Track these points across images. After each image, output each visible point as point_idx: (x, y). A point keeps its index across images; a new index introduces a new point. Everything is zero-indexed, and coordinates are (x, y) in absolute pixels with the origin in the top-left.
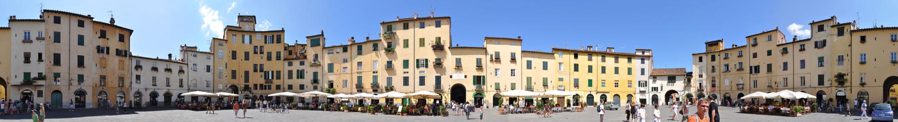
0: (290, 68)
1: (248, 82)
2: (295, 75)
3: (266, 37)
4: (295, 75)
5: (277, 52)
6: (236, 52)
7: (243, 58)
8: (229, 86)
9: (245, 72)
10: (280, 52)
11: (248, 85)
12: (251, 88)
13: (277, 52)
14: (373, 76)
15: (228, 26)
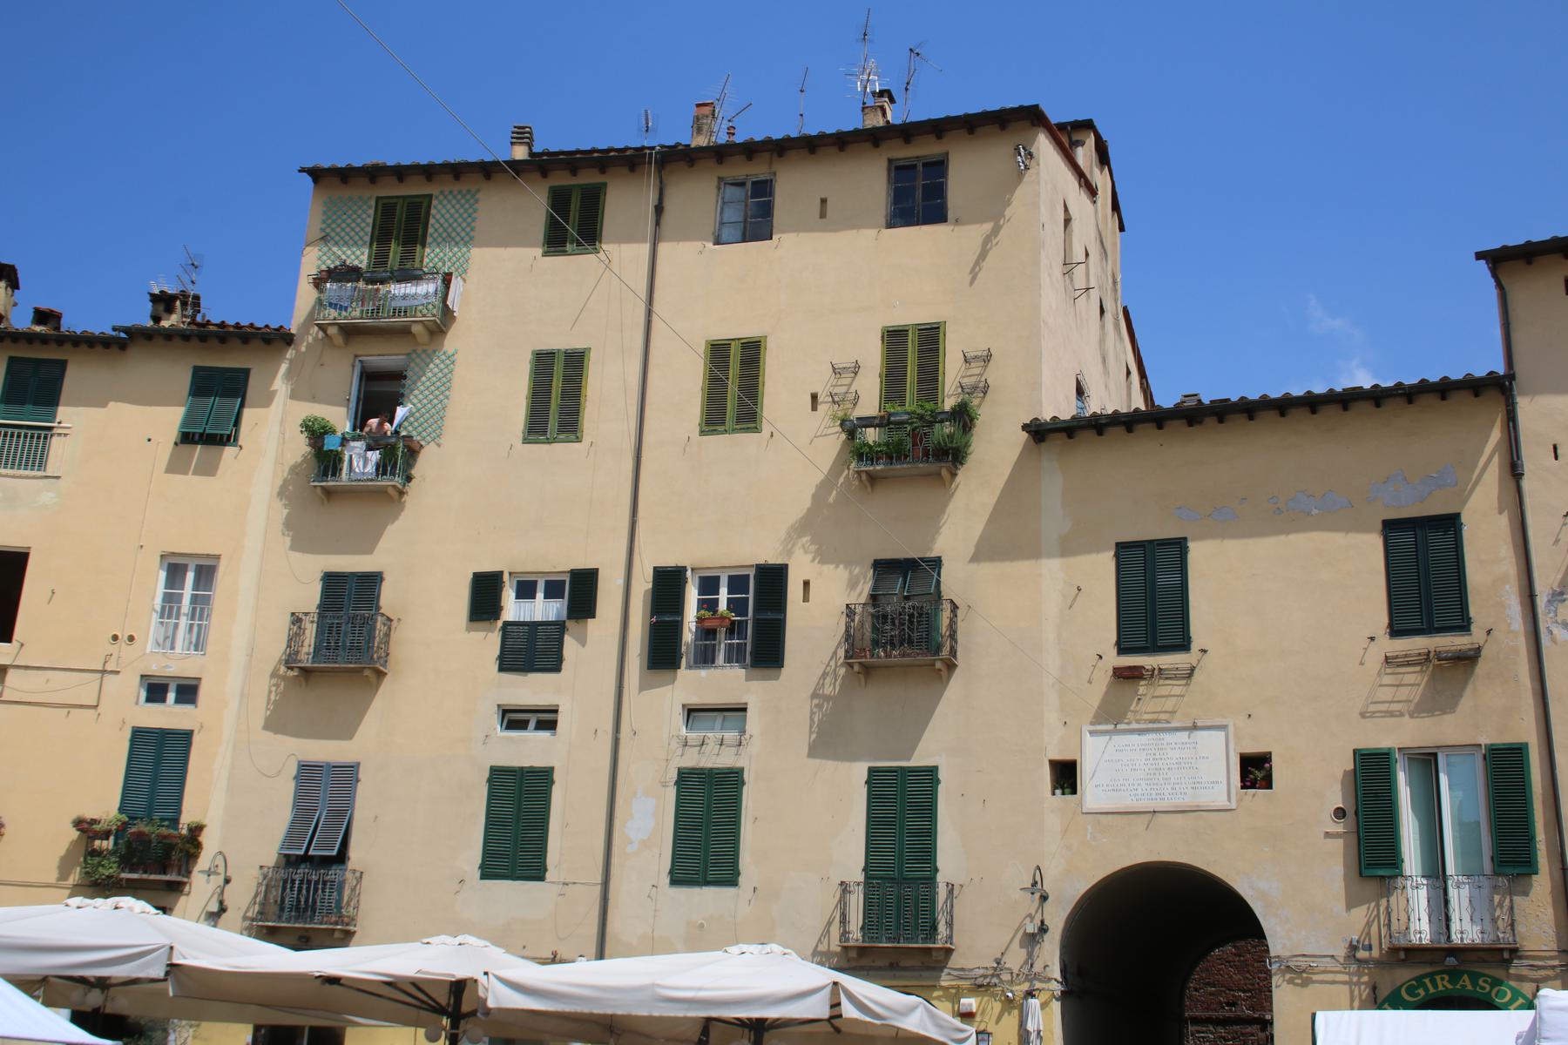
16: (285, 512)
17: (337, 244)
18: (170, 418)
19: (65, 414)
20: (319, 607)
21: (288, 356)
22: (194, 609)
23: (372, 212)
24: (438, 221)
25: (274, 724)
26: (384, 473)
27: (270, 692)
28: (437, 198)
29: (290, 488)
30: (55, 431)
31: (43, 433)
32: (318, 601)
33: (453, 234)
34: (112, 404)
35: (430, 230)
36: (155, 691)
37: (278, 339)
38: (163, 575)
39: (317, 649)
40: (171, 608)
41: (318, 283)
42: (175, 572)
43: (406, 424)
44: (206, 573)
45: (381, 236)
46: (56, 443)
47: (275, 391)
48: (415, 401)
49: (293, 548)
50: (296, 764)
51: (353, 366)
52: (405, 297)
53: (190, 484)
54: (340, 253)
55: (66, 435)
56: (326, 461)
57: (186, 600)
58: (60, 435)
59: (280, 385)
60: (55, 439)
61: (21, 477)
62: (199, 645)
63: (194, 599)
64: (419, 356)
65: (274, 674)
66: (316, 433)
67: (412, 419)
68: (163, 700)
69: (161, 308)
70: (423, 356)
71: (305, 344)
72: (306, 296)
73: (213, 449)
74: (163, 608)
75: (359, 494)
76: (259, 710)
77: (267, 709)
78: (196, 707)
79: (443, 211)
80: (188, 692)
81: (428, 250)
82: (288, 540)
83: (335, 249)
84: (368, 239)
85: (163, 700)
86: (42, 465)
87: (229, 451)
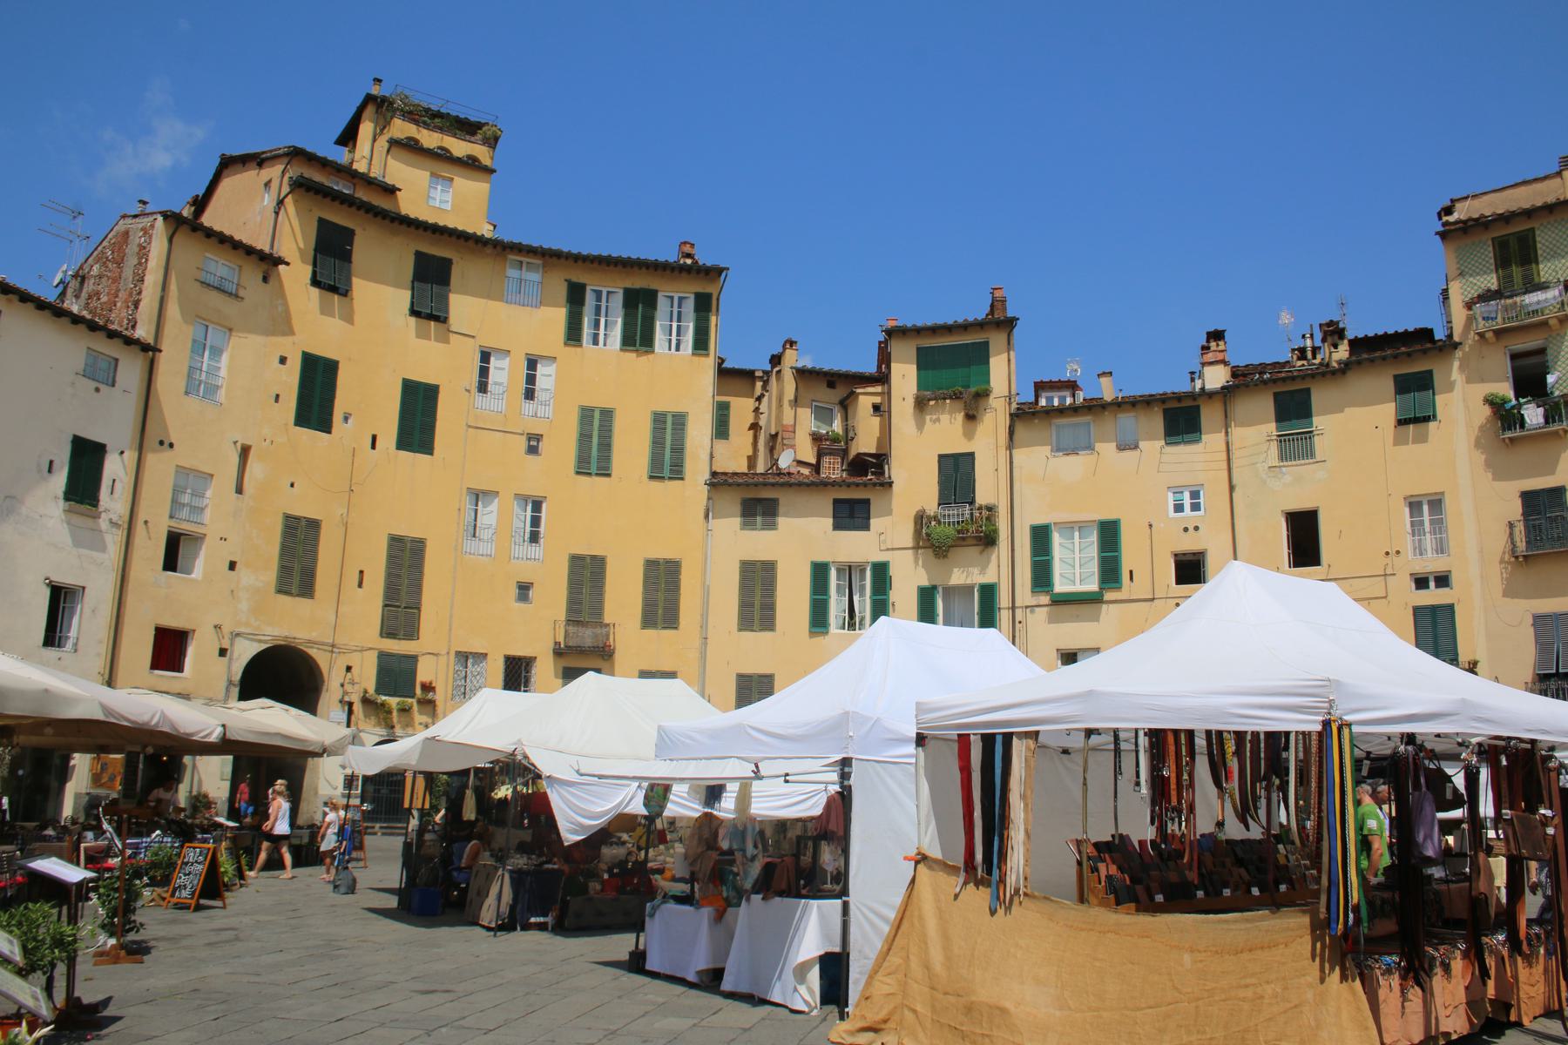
0: (759, 544)
1: (412, 632)
2: (793, 596)
3: (576, 296)
4: (793, 596)
5: (659, 419)
6: (331, 367)
7: (389, 427)
8: (245, 652)
9: (396, 542)
10: (680, 420)
11: (413, 659)
12: (428, 688)
13: (659, 419)
14: (1417, 611)
15: (296, 154)
16: (1483, 457)
17: (1471, 275)
18: (1387, 412)
19: (1316, 420)
20: (1523, 514)
21: (1457, 356)
22: (1435, 528)
23: (1491, 249)
24: (1544, 245)
25: (1509, 592)
26: (1554, 421)
27: (1502, 573)
28: (1538, 229)
29: (1483, 441)
30: (1315, 433)
31: (1308, 435)
32: (1521, 511)
33: (1559, 251)
34: (1346, 409)
35: (1540, 252)
36: (1421, 583)
37: (1450, 345)
38: (1407, 510)
39: (1528, 543)
40: (1419, 530)
41: (1469, 305)
42: (1414, 506)
43: (1557, 385)
44: (1436, 504)
45: (1503, 262)
46: (1316, 439)
47: (1455, 381)
48: (1560, 369)
49: (1494, 479)
50: (1531, 616)
51: (1505, 353)
52: (1538, 302)
53: (1411, 450)
54: (1475, 281)
55: (1322, 434)
56: (1505, 417)
57: (1427, 524)
58: (1318, 435)
59: (1456, 375)
60: (1316, 438)
61: (1301, 465)
62: (1441, 549)
63: (1432, 522)
64: (1554, 338)
65: (1502, 561)
66: (1496, 404)
67: (1561, 382)
68: (1428, 587)
69: (1336, 337)
70: (1558, 338)
71: (1467, 346)
72: (1459, 315)
73: (1421, 426)
74: (1413, 531)
75: (1538, 437)
76: (1497, 586)
77: (1503, 584)
78: (1452, 589)
79: (1547, 237)
80: (1443, 580)
81: (1541, 266)
82: (1490, 475)
83: (1471, 279)
84: (1493, 267)
85: (1428, 587)
86: (1312, 455)
87: (1432, 425)
